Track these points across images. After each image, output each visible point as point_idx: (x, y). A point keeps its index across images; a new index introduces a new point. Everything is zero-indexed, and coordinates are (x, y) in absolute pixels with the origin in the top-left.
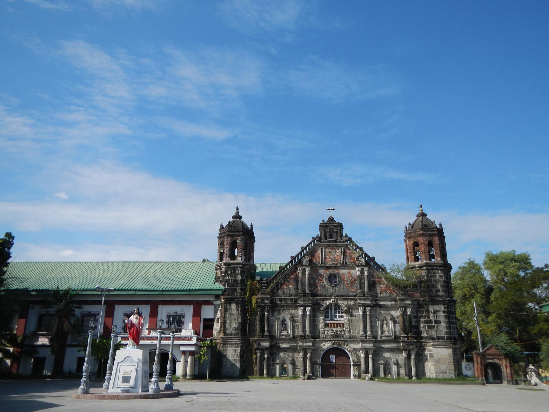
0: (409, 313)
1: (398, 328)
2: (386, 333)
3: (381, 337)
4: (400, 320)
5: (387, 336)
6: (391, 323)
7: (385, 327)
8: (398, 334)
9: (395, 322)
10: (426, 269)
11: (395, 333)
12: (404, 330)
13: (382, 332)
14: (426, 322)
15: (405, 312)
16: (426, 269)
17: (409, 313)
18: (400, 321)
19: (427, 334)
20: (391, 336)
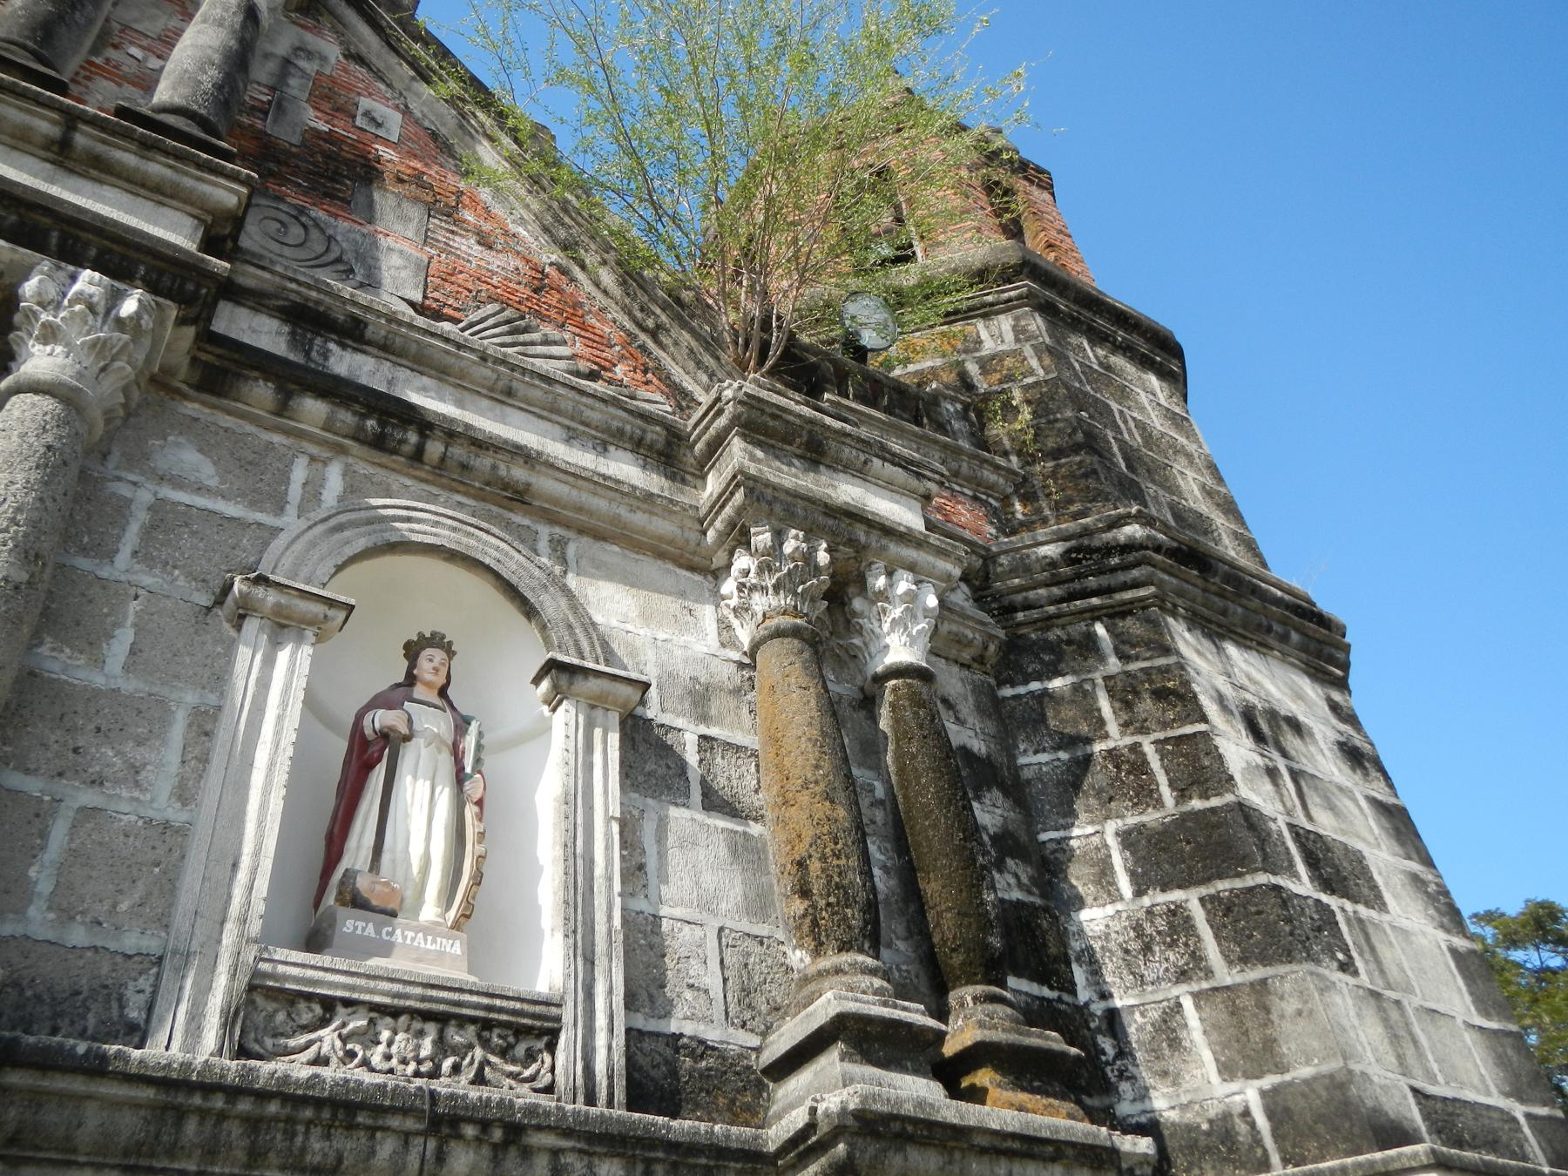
0: (899, 647)
1: (709, 886)
2: (425, 949)
3: (264, 1009)
4: (764, 734)
5: (434, 1014)
6: (556, 767)
7: (419, 808)
8: (700, 1015)
9: (649, 759)
10: (1028, 299)
11: (646, 988)
12: (850, 916)
13: (330, 887)
14: (1160, 858)
15: (828, 624)
16: (1028, 299)
17: (899, 647)
18: (736, 777)
19: (1249, 1050)
20: (526, 1029)
